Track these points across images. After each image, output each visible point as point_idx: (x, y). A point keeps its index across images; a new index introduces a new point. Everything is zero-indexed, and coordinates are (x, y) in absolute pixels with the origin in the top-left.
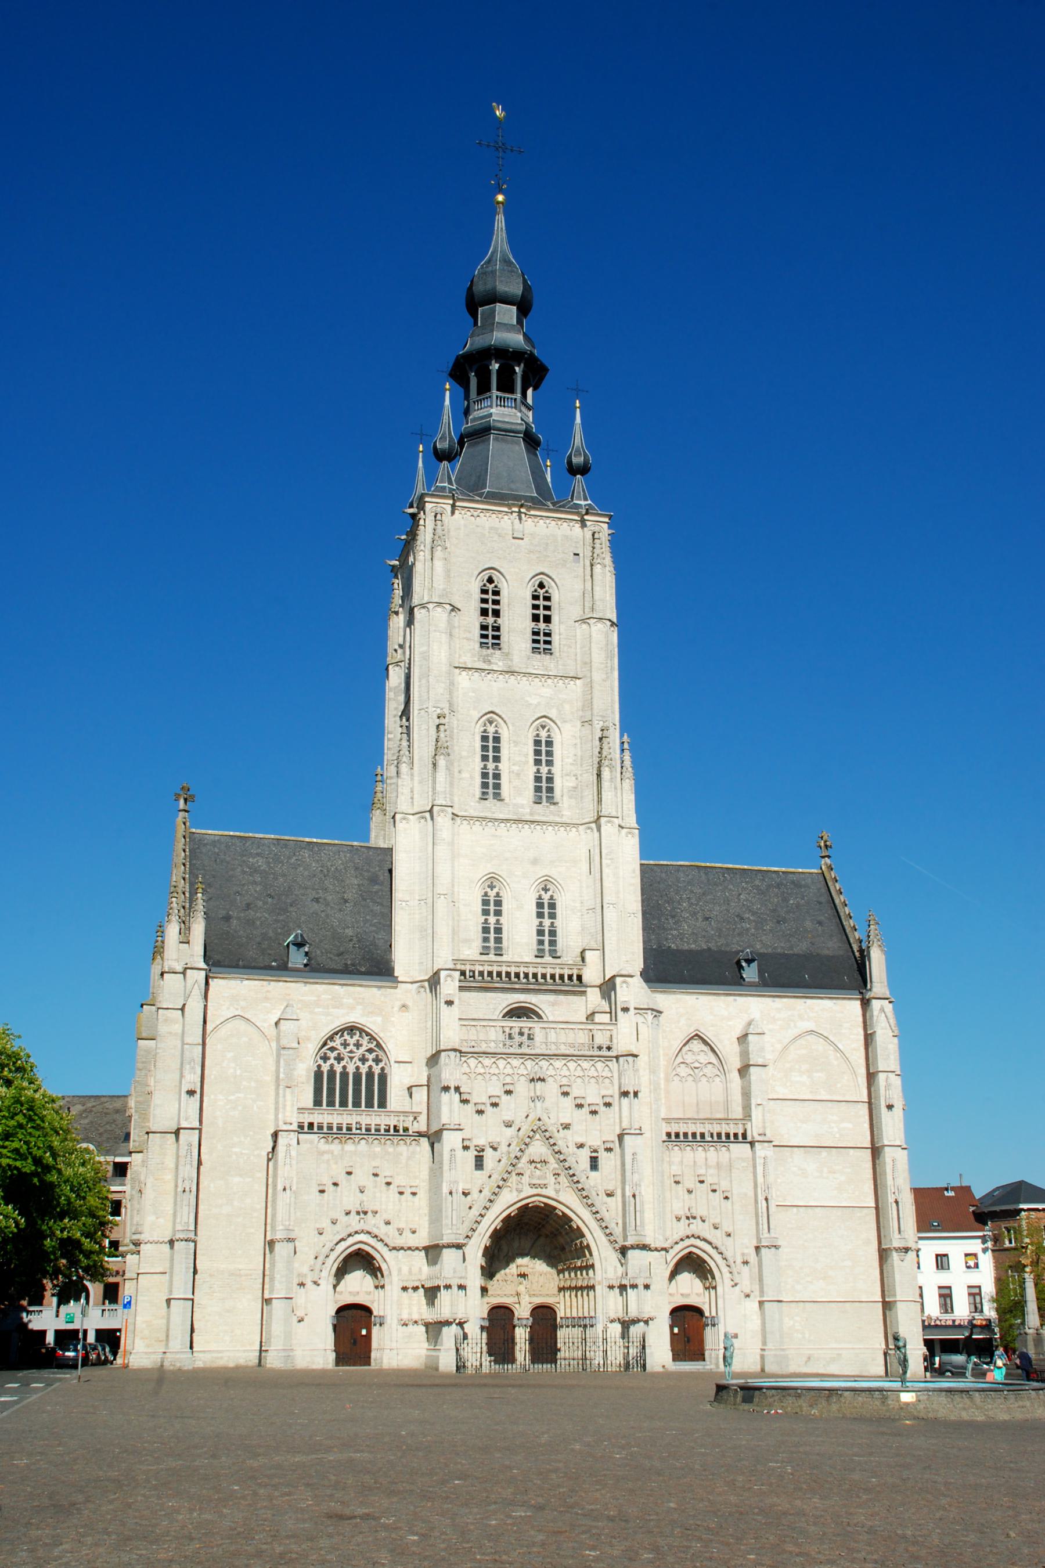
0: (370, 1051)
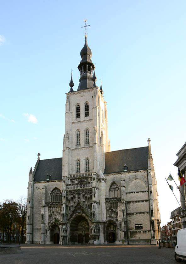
0: (59, 192)
